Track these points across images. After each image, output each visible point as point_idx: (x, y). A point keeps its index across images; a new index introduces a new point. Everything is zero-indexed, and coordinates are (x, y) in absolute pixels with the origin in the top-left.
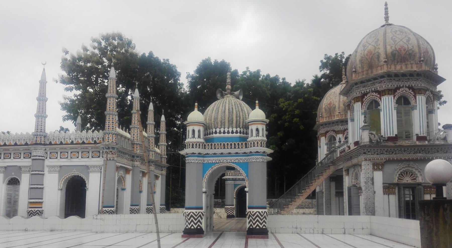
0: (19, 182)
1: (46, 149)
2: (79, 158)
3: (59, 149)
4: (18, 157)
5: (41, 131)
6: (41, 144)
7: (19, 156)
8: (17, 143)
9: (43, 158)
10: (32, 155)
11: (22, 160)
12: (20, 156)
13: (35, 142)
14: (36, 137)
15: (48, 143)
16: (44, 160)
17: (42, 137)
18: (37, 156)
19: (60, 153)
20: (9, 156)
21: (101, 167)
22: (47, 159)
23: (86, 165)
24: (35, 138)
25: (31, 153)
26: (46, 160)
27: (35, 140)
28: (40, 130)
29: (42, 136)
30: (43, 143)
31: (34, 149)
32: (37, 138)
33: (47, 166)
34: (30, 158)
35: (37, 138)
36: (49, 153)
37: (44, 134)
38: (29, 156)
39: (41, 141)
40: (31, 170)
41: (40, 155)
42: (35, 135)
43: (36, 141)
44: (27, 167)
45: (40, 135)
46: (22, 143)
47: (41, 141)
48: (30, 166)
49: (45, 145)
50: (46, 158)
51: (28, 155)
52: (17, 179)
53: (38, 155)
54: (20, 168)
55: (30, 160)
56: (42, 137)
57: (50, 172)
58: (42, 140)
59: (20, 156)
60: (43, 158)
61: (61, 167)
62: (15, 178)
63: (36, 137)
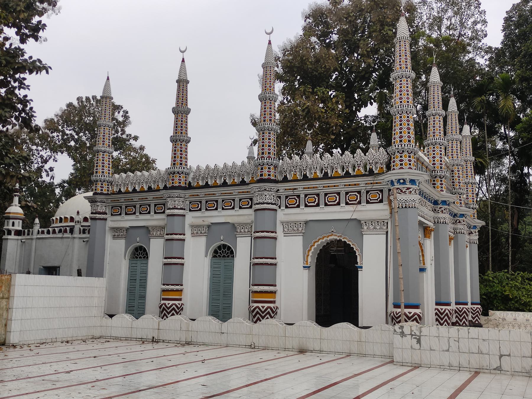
0: (232, 252)
1: (278, 190)
2: (341, 205)
3: (302, 190)
4: (230, 207)
5: (269, 157)
6: (269, 181)
7: (231, 205)
8: (227, 181)
9: (274, 207)
10: (255, 201)
11: (238, 212)
12: (233, 204)
13: (259, 178)
14: (260, 167)
15: (280, 178)
16: (276, 210)
17: (272, 167)
18: (264, 203)
19: (304, 196)
20: (214, 206)
21: (386, 221)
22: (282, 208)
23: (356, 219)
24: (260, 170)
25: (251, 199)
26: (279, 211)
27: (259, 173)
28: (267, 155)
29: (272, 164)
30: (272, 178)
31: (258, 191)
32: (262, 169)
33: (282, 223)
34: (251, 207)
35: (262, 169)
36: (283, 198)
37: (275, 162)
38: (249, 204)
39: (269, 175)
40: (253, 231)
41: (270, 201)
42: (259, 165)
43: (261, 175)
44: (246, 224)
45: (268, 164)
46: (236, 181)
47: (269, 175)
48: (252, 222)
49: (276, 181)
50: (280, 207)
51: (249, 203)
52: (229, 248)
53: (265, 201)
54: (233, 226)
55: (250, 211)
56: (272, 167)
57: (286, 234)
58: (272, 173)
59: (233, 204)
60: (274, 207)
61: (306, 223)
62: (224, 246)
63: (260, 167)
